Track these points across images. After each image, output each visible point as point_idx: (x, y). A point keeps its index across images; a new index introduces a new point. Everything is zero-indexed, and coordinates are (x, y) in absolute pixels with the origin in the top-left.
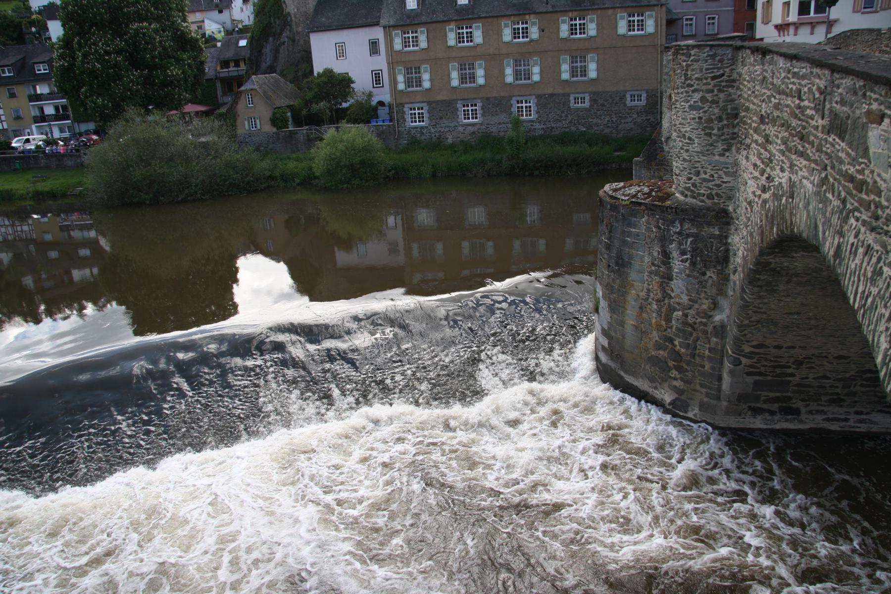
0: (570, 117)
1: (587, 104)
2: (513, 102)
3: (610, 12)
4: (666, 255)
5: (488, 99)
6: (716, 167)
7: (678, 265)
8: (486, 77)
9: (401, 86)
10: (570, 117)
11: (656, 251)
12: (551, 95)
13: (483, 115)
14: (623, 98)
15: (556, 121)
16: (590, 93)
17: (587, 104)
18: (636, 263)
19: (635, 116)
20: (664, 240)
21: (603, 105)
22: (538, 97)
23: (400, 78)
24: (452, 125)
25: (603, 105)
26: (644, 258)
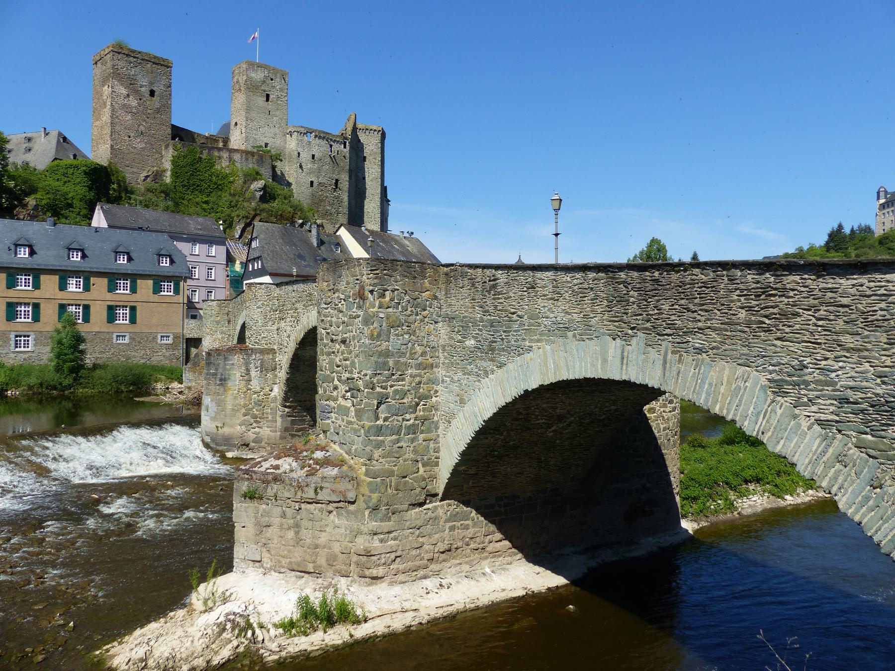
0: (113, 350)
1: (127, 340)
4: (248, 370)
7: (254, 373)
10: (113, 350)
13: (35, 345)
14: (155, 338)
15: (101, 353)
16: (130, 333)
17: (127, 340)
18: (232, 378)
19: (164, 351)
20: (247, 364)
21: (139, 342)
24: (4, 352)
25: (139, 342)
26: (236, 375)
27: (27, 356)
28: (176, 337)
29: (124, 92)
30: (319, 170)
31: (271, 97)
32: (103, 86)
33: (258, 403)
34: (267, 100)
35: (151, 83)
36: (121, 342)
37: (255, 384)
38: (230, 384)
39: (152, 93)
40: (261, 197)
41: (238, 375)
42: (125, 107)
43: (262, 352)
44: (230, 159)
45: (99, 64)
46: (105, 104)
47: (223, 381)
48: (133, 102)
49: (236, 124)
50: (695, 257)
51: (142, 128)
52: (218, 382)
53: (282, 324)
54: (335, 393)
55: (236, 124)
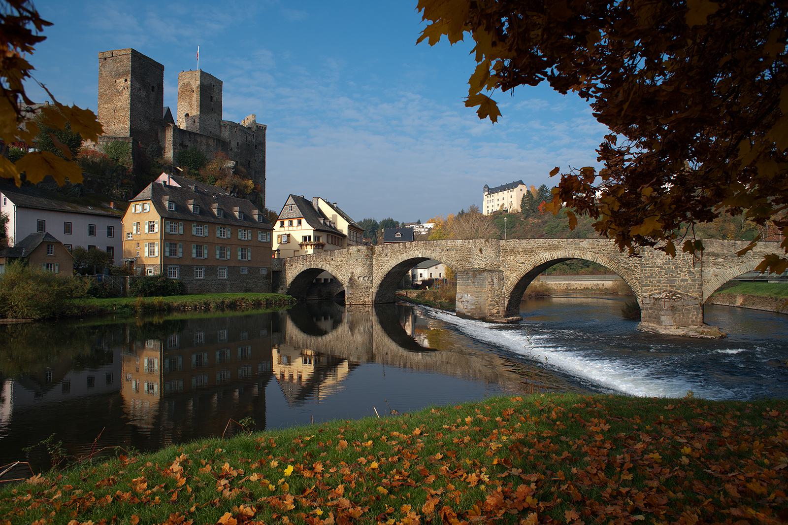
1: (246, 273)
2: (218, 269)
3: (256, 230)
4: (492, 280)
5: (208, 266)
6: (497, 261)
7: (495, 281)
8: (208, 254)
9: (167, 254)
12: (234, 267)
13: (205, 275)
14: (259, 270)
15: (235, 280)
17: (246, 273)
22: (228, 267)
23: (167, 249)
27: (200, 283)
29: (138, 86)
32: (119, 78)
33: (497, 295)
36: (244, 273)
37: (496, 286)
44: (208, 145)
45: (109, 61)
46: (120, 93)
48: (143, 95)
53: (512, 257)
54: (678, 276)
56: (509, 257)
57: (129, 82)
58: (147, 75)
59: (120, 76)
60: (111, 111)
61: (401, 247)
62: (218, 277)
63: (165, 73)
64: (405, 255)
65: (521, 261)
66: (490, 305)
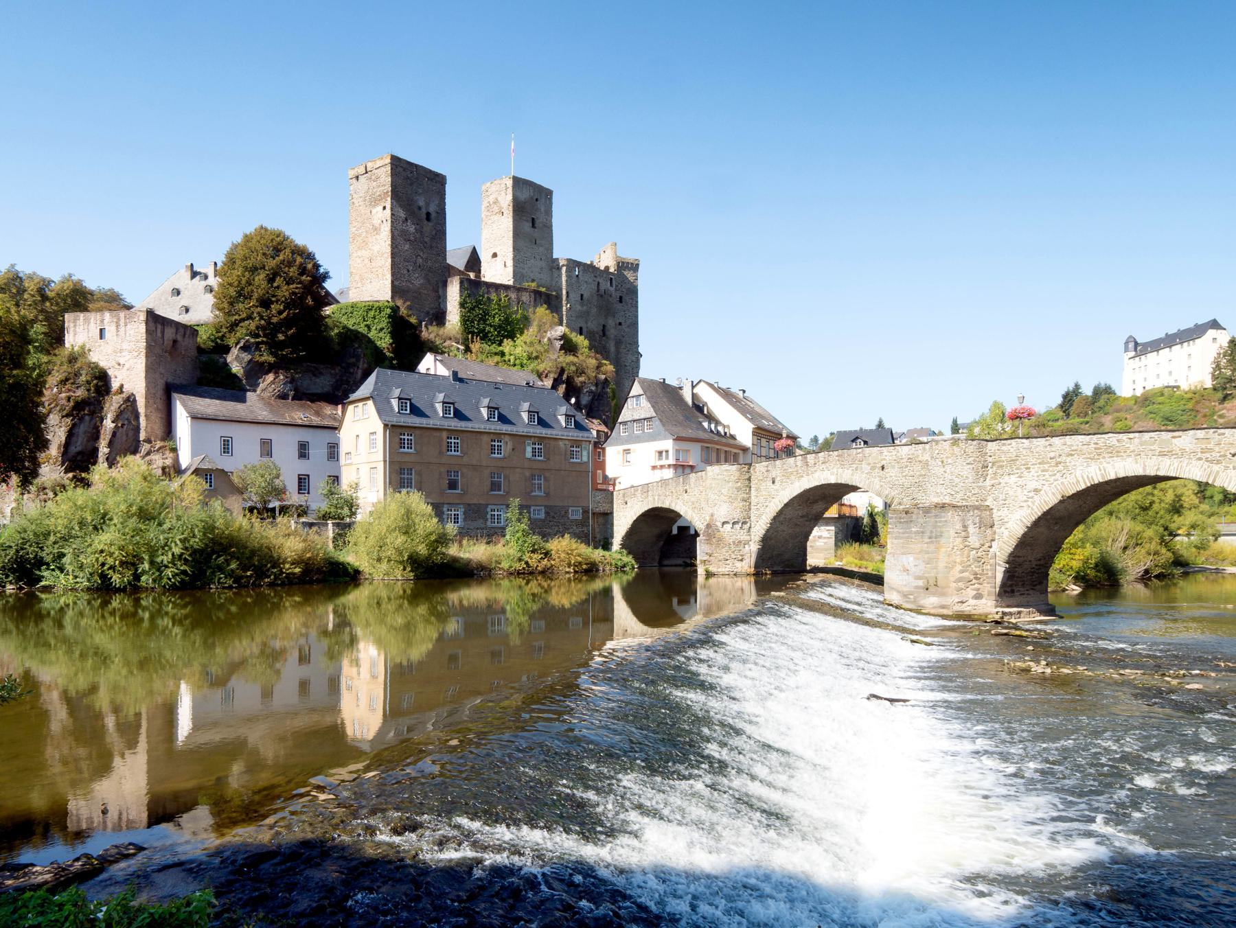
1: (542, 516)
4: (965, 527)
7: (971, 529)
11: (958, 526)
13: (465, 520)
14: (567, 512)
18: (946, 535)
28: (585, 512)
29: (402, 214)
30: (587, 313)
31: (537, 222)
32: (374, 206)
33: (978, 560)
34: (533, 226)
35: (428, 204)
37: (974, 541)
38: (943, 540)
39: (428, 214)
40: (562, 348)
41: (952, 533)
42: (404, 234)
43: (977, 508)
46: (376, 230)
47: (935, 537)
48: (412, 229)
49: (495, 255)
50: (880, 425)
51: (420, 260)
52: (927, 540)
55: (495, 255)
56: (1007, 477)
57: (388, 211)
58: (417, 197)
59: (374, 201)
60: (367, 261)
61: (799, 463)
62: (489, 523)
63: (449, 189)
64: (805, 479)
65: (1032, 485)
66: (959, 580)
